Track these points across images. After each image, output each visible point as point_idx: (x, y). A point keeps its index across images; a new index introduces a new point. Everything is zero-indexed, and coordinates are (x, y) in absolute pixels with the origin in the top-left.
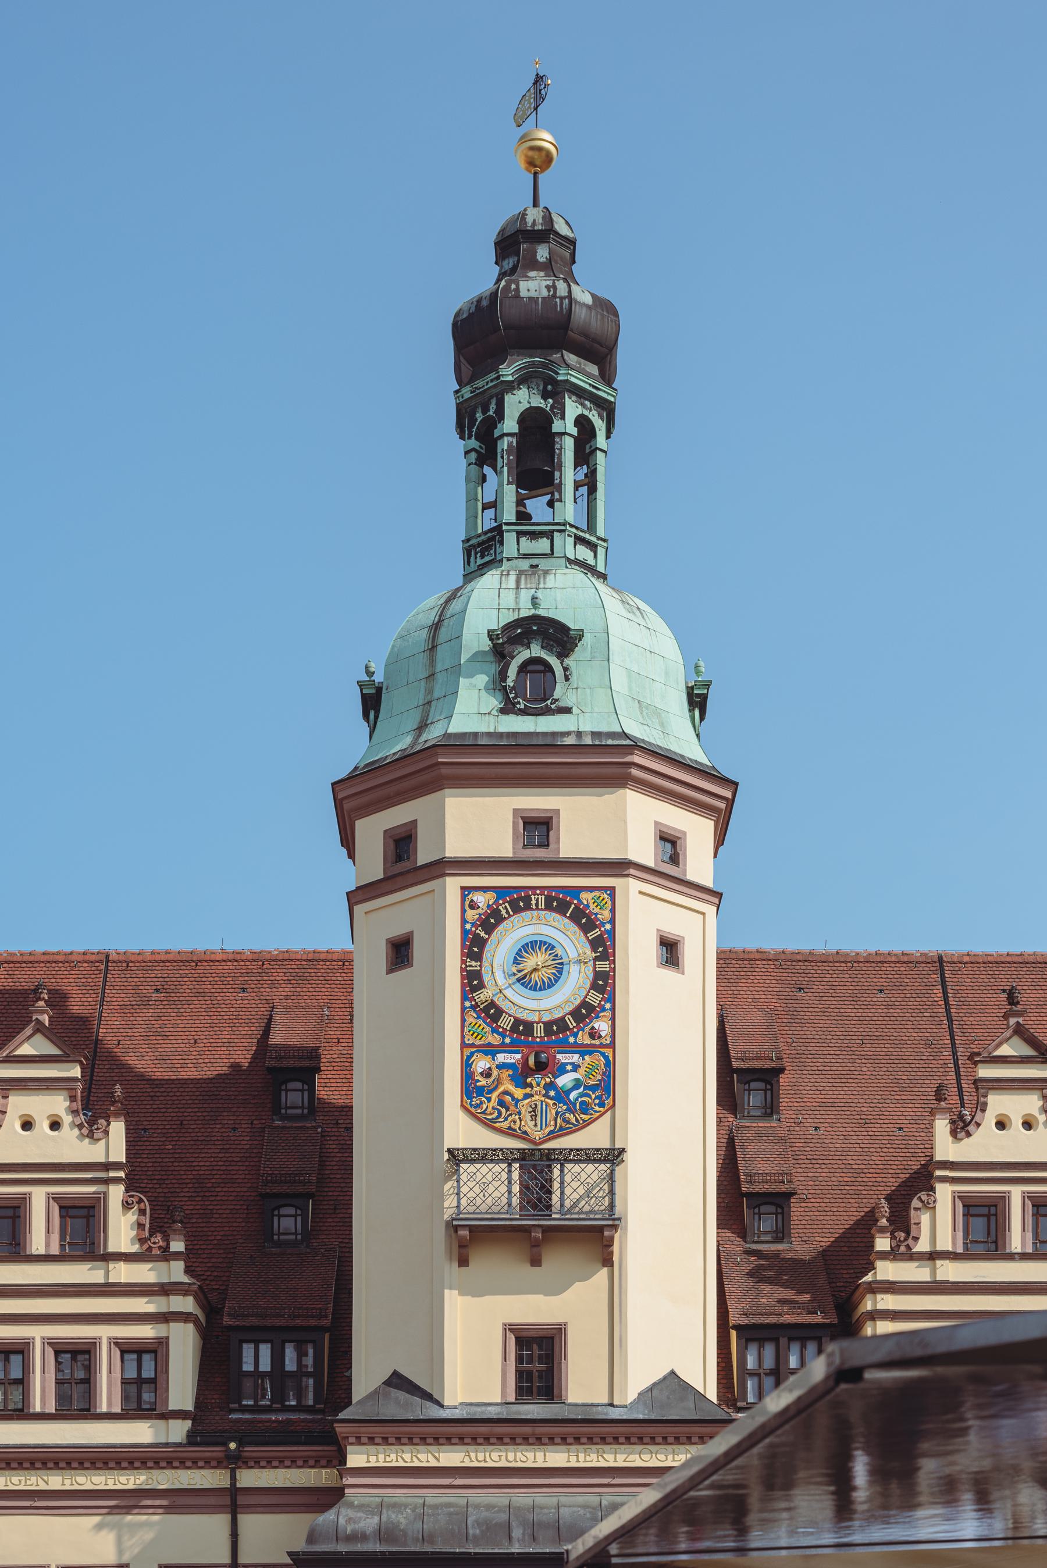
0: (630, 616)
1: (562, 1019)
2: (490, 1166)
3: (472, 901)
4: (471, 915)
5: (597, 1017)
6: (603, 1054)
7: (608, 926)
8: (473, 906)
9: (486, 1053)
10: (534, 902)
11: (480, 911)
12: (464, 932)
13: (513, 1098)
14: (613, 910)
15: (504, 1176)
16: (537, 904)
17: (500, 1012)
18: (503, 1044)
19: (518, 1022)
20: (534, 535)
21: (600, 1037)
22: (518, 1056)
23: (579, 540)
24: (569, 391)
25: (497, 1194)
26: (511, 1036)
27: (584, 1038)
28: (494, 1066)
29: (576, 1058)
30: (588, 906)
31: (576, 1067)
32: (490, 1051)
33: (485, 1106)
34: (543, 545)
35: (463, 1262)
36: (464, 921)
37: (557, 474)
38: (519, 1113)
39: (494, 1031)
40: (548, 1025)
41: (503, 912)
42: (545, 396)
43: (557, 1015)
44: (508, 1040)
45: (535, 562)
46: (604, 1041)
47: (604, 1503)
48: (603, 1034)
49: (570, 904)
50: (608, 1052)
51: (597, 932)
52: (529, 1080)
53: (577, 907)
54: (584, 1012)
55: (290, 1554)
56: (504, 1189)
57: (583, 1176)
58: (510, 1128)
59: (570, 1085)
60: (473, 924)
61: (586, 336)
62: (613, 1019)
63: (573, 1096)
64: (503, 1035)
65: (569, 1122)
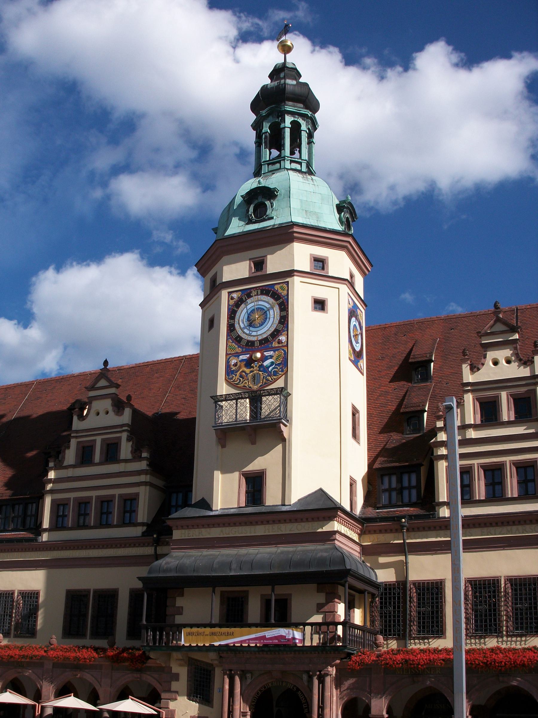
0: (304, 181)
1: (267, 338)
4: (232, 302)
6: (283, 350)
8: (232, 298)
9: (235, 356)
11: (235, 300)
13: (246, 373)
15: (235, 405)
22: (248, 356)
23: (292, 162)
29: (271, 353)
31: (271, 357)
32: (237, 355)
34: (278, 166)
35: (223, 446)
37: (283, 141)
38: (248, 379)
41: (244, 298)
43: (265, 336)
44: (244, 350)
48: (283, 341)
50: (285, 349)
51: (281, 300)
54: (276, 334)
55: (140, 579)
58: (244, 386)
59: (269, 365)
63: (270, 369)
64: (242, 348)
65: (268, 380)
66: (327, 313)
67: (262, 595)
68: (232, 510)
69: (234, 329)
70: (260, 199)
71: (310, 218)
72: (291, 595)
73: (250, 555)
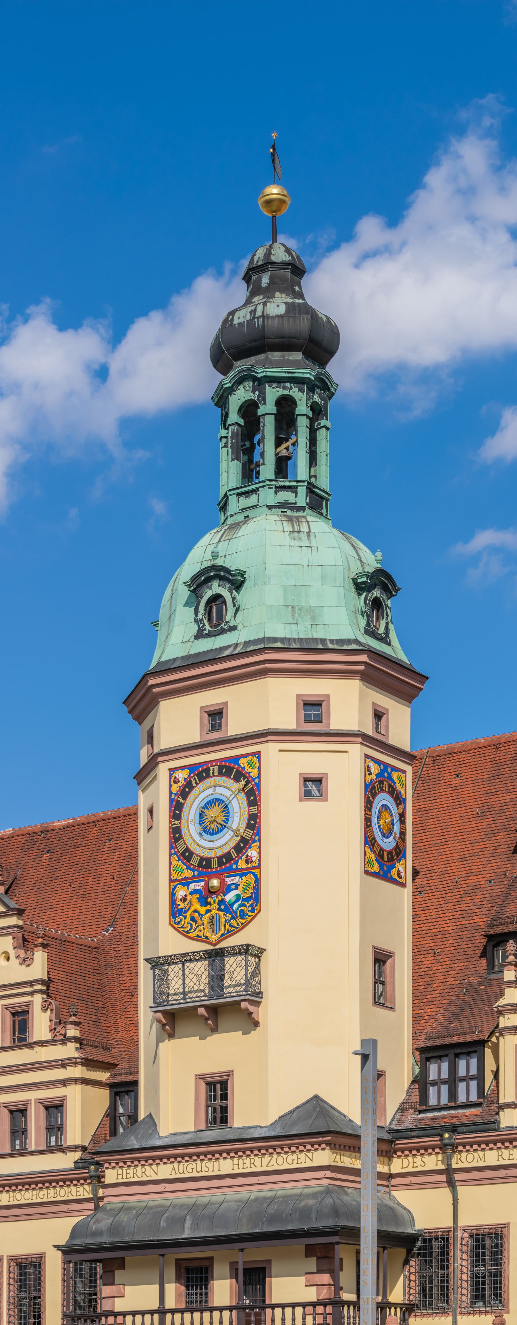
1: (229, 853)
2: (172, 967)
3: (175, 778)
4: (175, 788)
5: (250, 847)
6: (253, 874)
7: (257, 781)
9: (183, 885)
10: (211, 772)
11: (180, 784)
12: (171, 800)
13: (200, 914)
14: (259, 769)
15: (181, 973)
16: (213, 773)
17: (192, 853)
18: (194, 877)
19: (202, 859)
20: (247, 494)
21: (252, 861)
22: (202, 884)
24: (268, 382)
25: (177, 986)
26: (198, 871)
27: (242, 864)
28: (188, 893)
29: (237, 879)
30: (244, 768)
31: (237, 886)
32: (185, 882)
33: (183, 922)
36: (171, 793)
38: (203, 924)
39: (188, 868)
40: (220, 858)
41: (194, 782)
42: (253, 391)
43: (226, 849)
44: (196, 873)
45: (246, 513)
46: (254, 865)
47: (252, 1197)
48: (254, 859)
49: (233, 768)
50: (256, 871)
52: (209, 900)
53: (237, 770)
54: (242, 845)
56: (181, 982)
57: (196, 969)
58: (198, 936)
59: (233, 900)
60: (176, 794)
61: (282, 337)
62: (260, 847)
65: (232, 926)
66: (327, 800)
67: (231, 1263)
68: (187, 1136)
69: (181, 837)
70: (216, 588)
71: (300, 621)
72: (269, 1262)
73: (212, 1204)
